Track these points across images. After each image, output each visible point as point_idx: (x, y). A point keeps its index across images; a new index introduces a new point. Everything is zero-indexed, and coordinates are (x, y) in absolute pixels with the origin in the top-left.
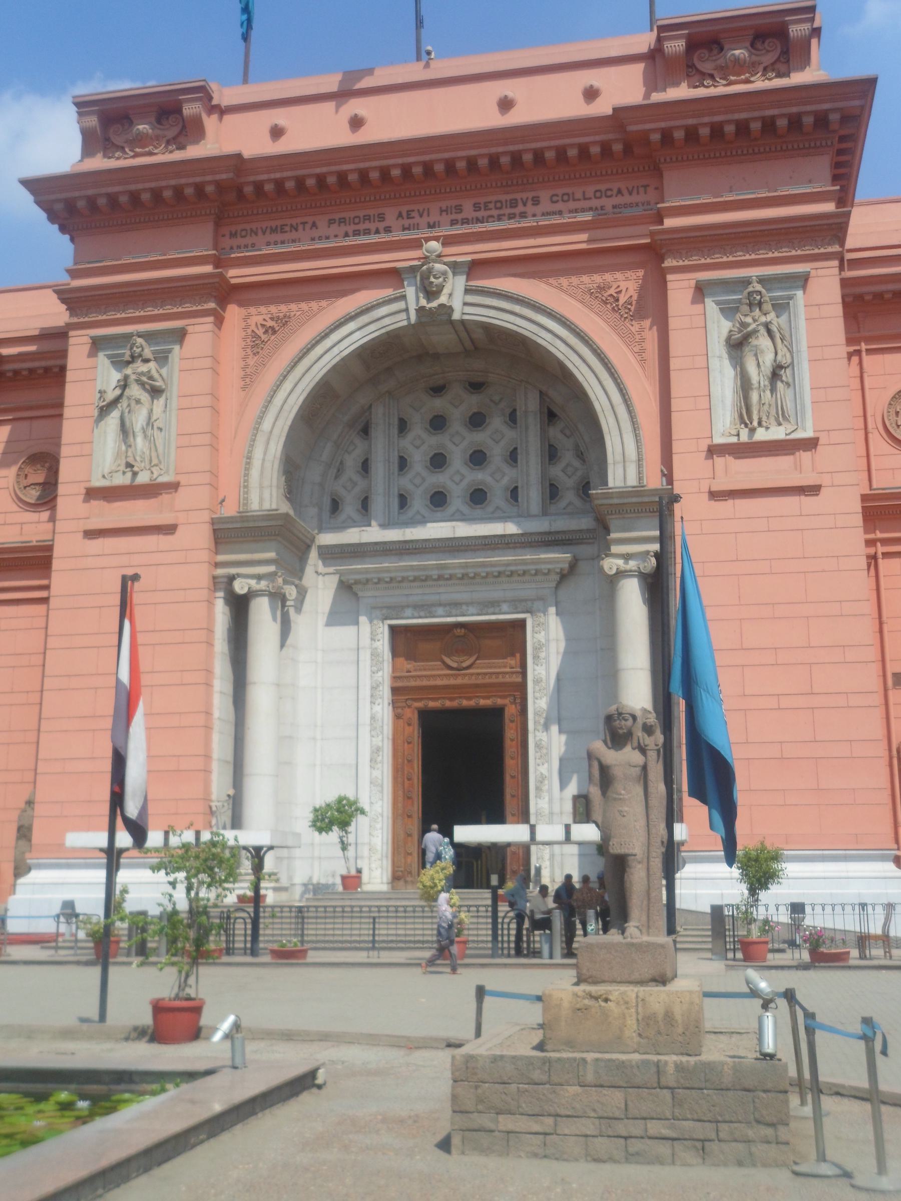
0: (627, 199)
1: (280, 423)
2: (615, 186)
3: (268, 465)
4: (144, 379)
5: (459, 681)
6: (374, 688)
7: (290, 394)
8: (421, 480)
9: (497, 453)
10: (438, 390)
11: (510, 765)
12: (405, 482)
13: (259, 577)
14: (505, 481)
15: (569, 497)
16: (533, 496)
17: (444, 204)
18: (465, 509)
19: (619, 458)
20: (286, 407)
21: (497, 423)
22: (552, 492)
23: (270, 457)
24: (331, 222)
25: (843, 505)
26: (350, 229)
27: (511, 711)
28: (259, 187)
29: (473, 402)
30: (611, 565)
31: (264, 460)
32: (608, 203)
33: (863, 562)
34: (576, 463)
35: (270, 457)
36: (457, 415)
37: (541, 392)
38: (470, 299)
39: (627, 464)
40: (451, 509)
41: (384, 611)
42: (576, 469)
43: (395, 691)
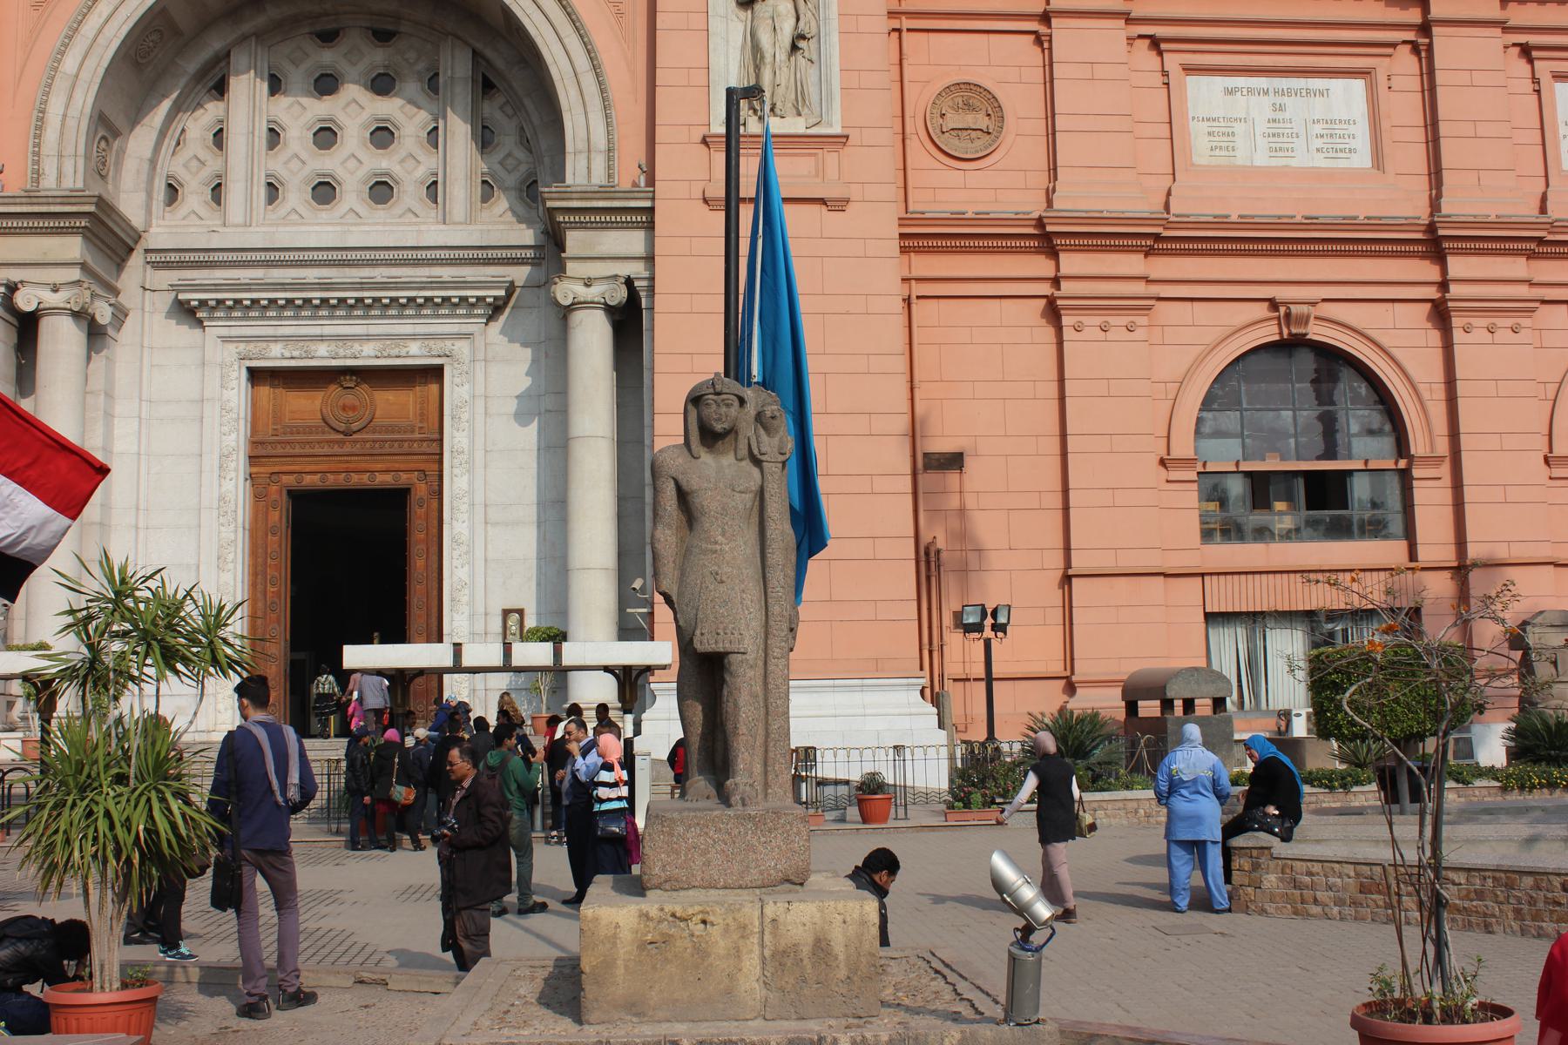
1: (91, 63)
3: (72, 123)
5: (347, 449)
6: (224, 457)
7: (107, 21)
8: (299, 162)
10: (328, 37)
11: (418, 563)
12: (277, 164)
13: (55, 289)
14: (421, 172)
16: (460, 191)
18: (362, 209)
19: (582, 145)
20: (100, 40)
22: (487, 189)
23: (74, 112)
27: (421, 490)
29: (377, 57)
30: (566, 291)
31: (65, 116)
33: (899, 305)
34: (520, 154)
35: (74, 112)
37: (475, 52)
39: (593, 155)
41: (242, 346)
42: (520, 163)
43: (253, 459)
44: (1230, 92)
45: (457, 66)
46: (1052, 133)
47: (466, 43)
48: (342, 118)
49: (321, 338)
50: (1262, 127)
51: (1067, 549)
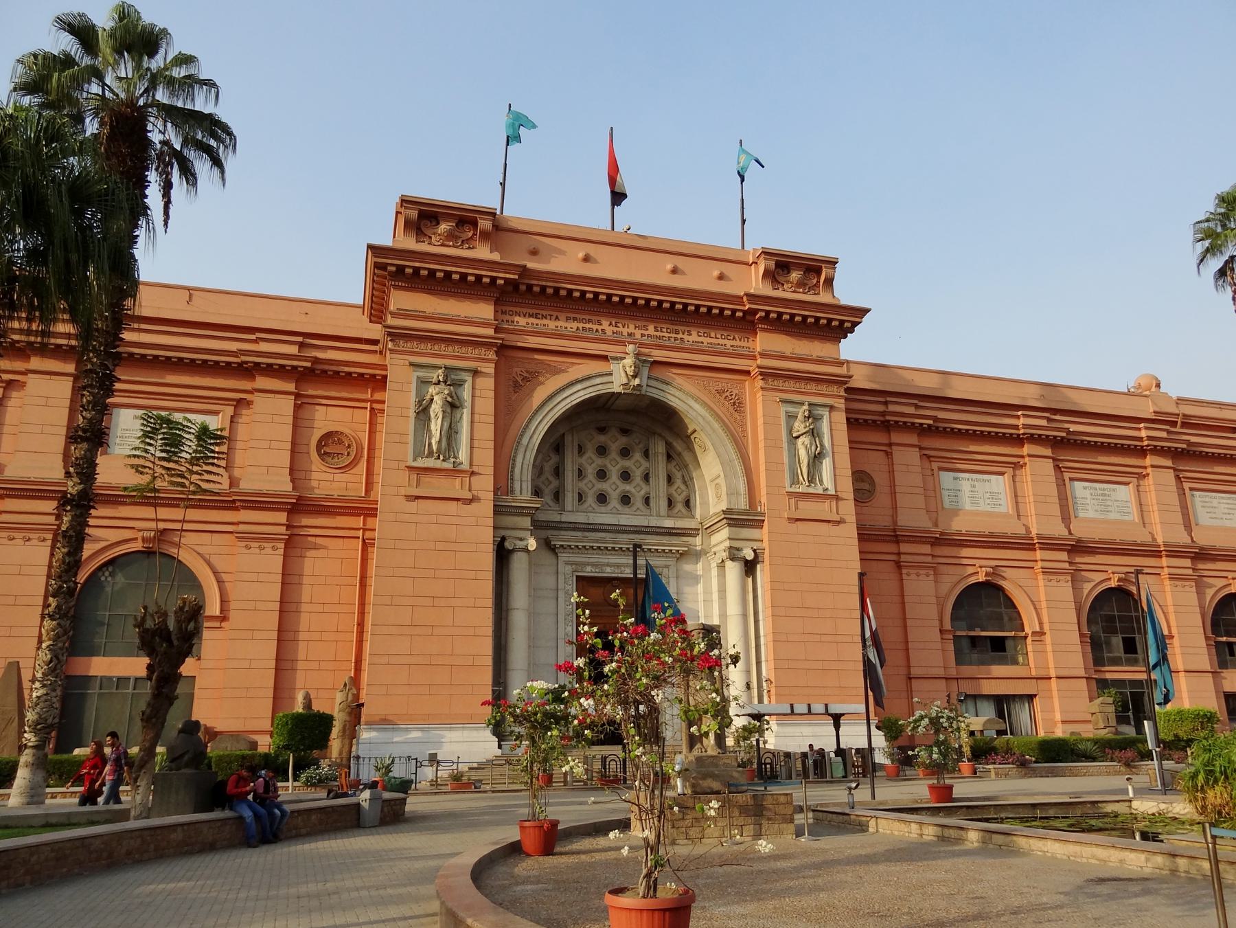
0: (737, 343)
2: (732, 334)
4: (449, 399)
8: (592, 486)
9: (637, 474)
10: (602, 430)
12: (582, 485)
13: (521, 539)
14: (643, 492)
15: (680, 507)
16: (663, 503)
17: (638, 323)
18: (619, 506)
21: (638, 456)
22: (670, 503)
23: (526, 462)
24: (568, 319)
25: (850, 531)
26: (581, 325)
28: (530, 287)
29: (623, 441)
32: (729, 343)
34: (683, 487)
36: (614, 447)
38: (652, 383)
40: (610, 507)
44: (956, 479)
45: (660, 448)
46: (893, 493)
47: (663, 438)
48: (609, 466)
49: (608, 565)
50: (967, 494)
51: (909, 667)
